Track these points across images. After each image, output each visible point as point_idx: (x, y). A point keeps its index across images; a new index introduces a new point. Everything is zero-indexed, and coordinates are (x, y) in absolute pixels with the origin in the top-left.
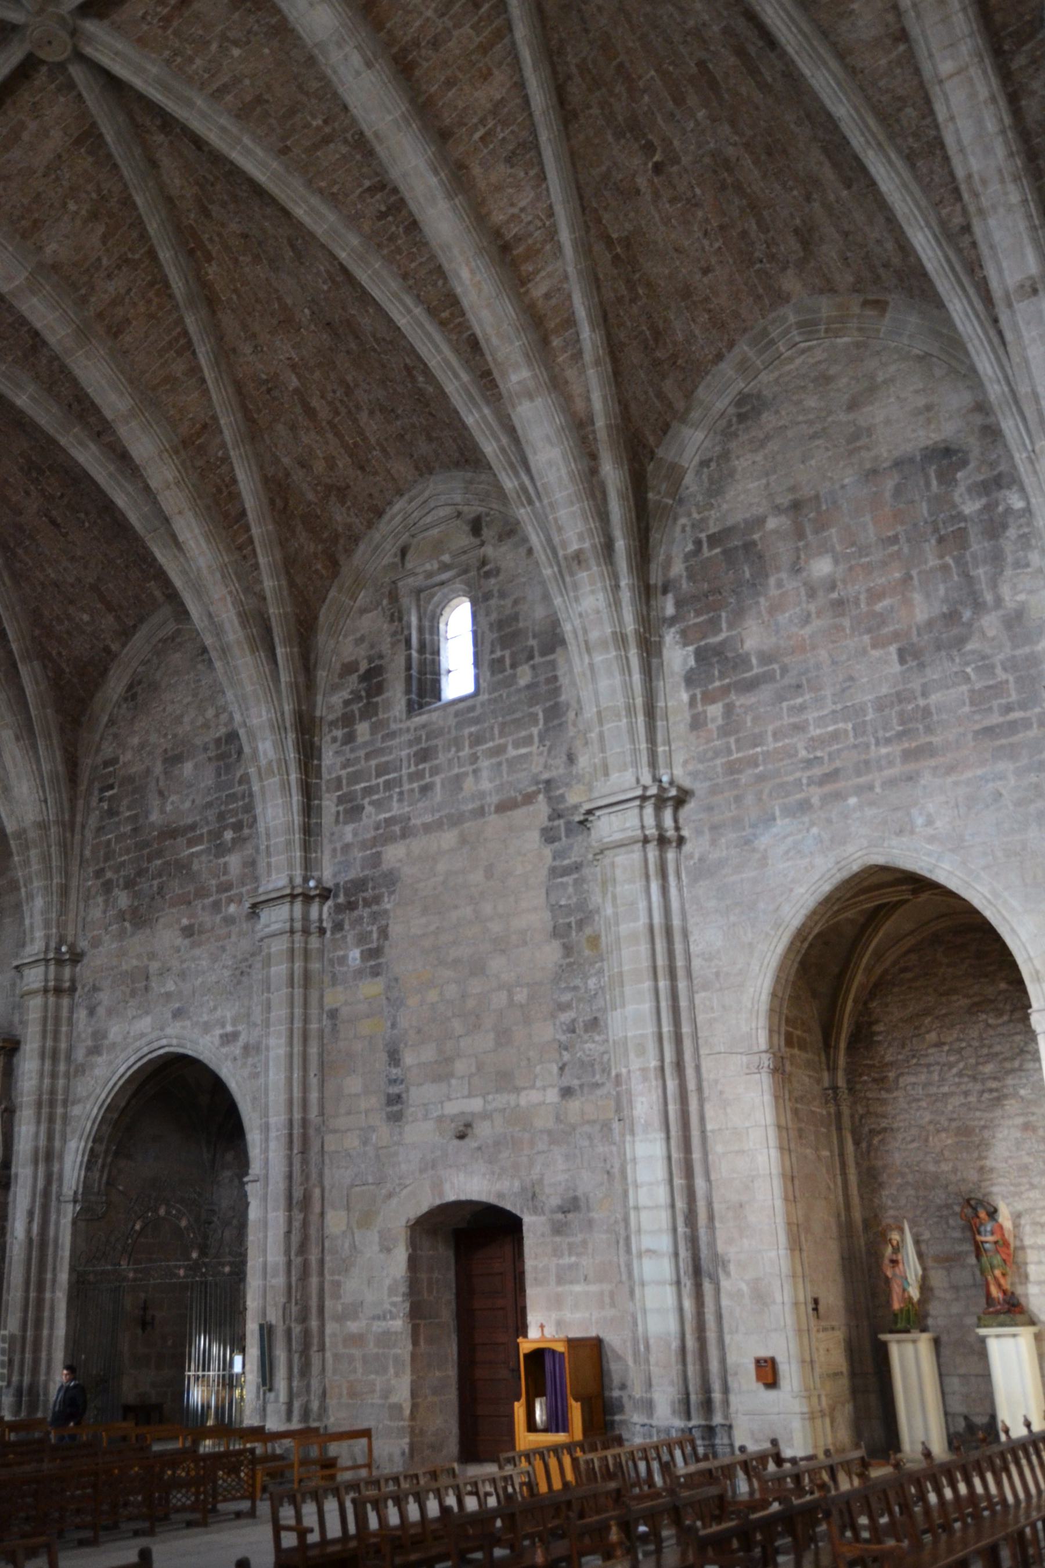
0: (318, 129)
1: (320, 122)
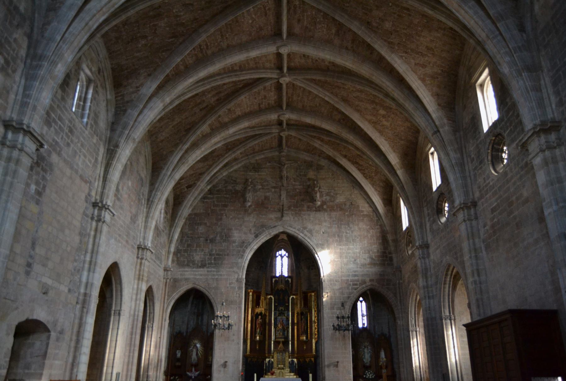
1: (227, 36)
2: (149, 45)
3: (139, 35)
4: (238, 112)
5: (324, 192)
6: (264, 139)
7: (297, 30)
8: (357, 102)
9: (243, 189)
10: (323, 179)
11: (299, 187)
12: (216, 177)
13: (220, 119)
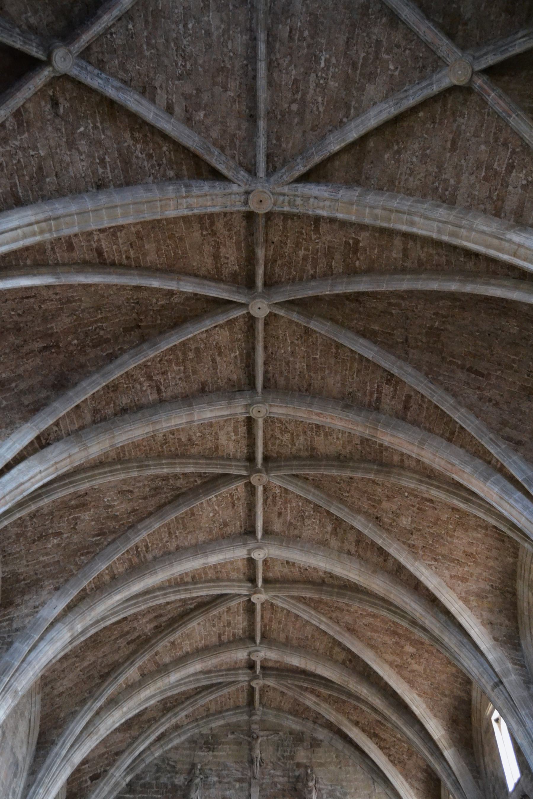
0: (175, 533)
2: (63, 545)
3: (50, 531)
4: (187, 648)
5: (323, 789)
6: (226, 691)
7: (277, 526)
8: (369, 633)
9: (186, 783)
10: (321, 765)
11: (281, 779)
12: (143, 760)
13: (157, 657)
